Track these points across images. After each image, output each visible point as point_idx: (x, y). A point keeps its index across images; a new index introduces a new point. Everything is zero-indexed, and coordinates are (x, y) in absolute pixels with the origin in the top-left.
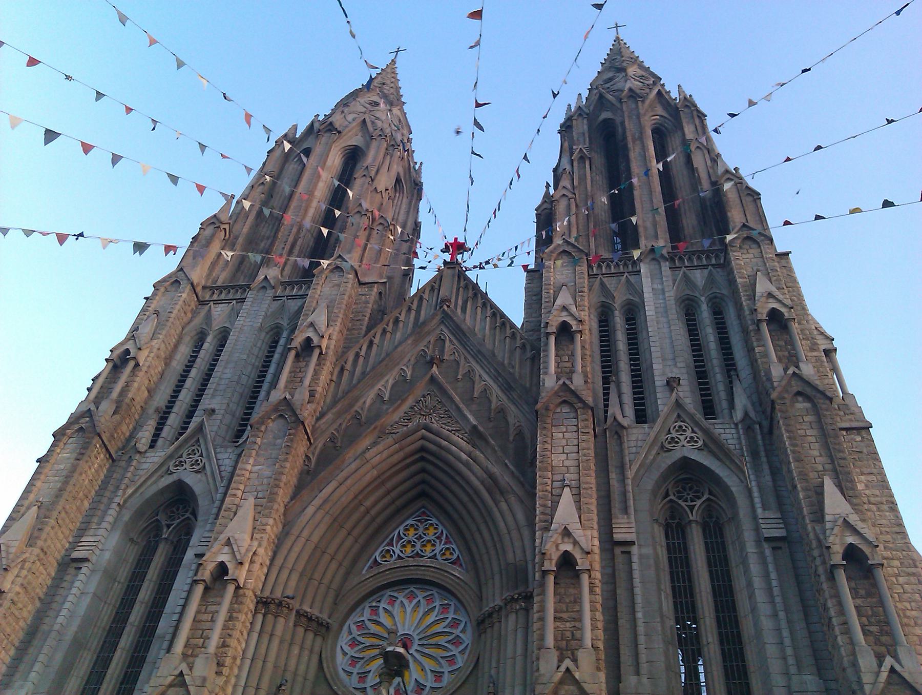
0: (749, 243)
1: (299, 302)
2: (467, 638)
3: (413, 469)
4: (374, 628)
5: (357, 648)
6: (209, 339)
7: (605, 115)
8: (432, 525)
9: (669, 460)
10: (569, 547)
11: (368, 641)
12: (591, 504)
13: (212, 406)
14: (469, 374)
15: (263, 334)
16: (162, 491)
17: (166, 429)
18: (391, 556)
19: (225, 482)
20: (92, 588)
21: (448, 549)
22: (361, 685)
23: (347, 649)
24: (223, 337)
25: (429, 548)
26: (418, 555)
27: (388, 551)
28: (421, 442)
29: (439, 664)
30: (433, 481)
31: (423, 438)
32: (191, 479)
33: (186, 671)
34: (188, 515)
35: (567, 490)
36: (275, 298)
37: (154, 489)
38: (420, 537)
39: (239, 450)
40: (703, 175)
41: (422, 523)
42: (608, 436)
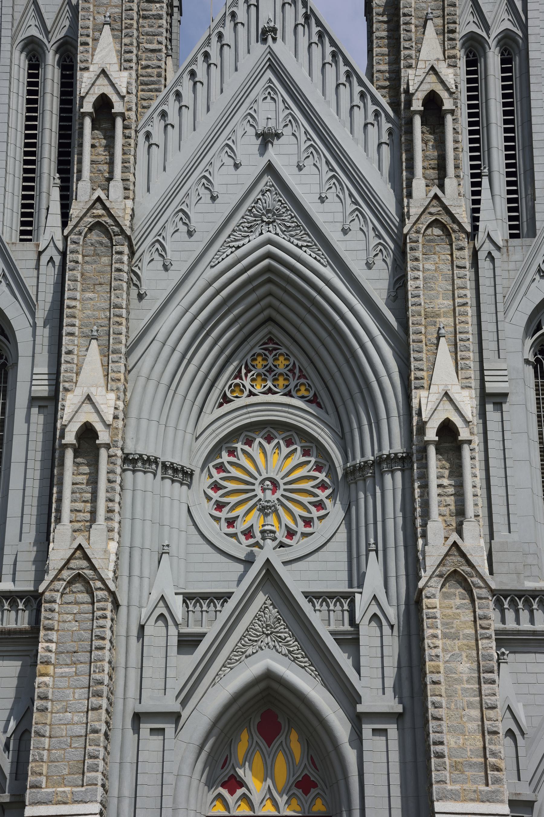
3: (261, 292)
4: (235, 472)
5: (221, 492)
8: (281, 354)
11: (231, 486)
12: (468, 359)
15: (16, 53)
18: (242, 391)
21: (302, 384)
22: (231, 530)
23: (210, 492)
25: (281, 382)
26: (270, 391)
27: (237, 385)
29: (309, 512)
30: (282, 307)
31: (269, 255)
33: (85, 545)
35: (442, 339)
38: (270, 370)
41: (270, 352)
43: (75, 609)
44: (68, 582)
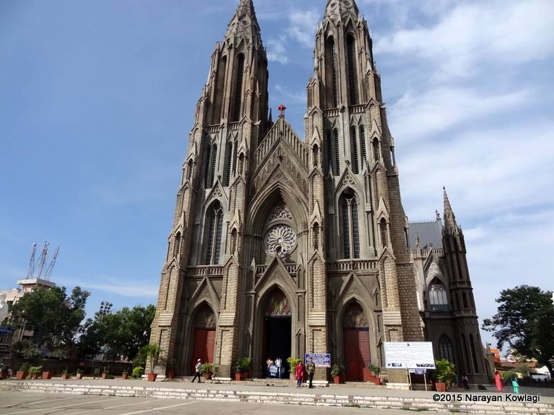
2: (295, 238)
7: (330, 33)
9: (344, 187)
10: (316, 221)
13: (218, 175)
14: (289, 161)
32: (219, 199)
36: (228, 131)
40: (363, 67)
42: (328, 183)
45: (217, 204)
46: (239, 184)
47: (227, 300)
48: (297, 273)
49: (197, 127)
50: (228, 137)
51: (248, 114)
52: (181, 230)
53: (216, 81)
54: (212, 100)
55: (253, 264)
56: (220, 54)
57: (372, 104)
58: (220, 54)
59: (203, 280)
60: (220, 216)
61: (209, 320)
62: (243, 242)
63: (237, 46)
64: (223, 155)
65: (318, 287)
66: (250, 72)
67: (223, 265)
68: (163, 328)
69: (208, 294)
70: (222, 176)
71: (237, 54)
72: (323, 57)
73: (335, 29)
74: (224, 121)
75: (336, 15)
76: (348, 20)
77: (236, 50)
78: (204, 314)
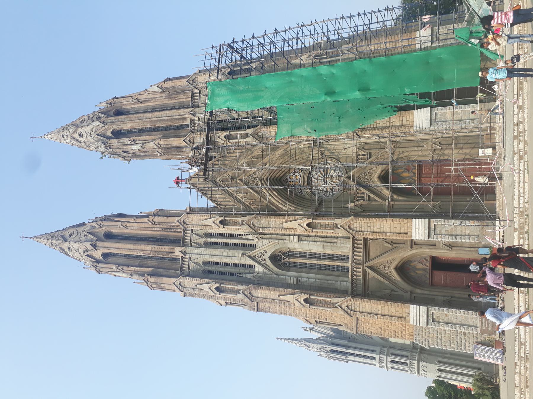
0: (195, 80)
1: (194, 236)
6: (207, 268)
7: (109, 133)
13: (240, 255)
16: (272, 263)
17: (246, 271)
19: (272, 240)
20: (305, 275)
24: (206, 263)
28: (265, 179)
32: (269, 254)
34: (281, 254)
36: (191, 246)
37: (272, 266)
39: (261, 239)
43: (358, 227)
44: (350, 229)
45: (274, 258)
46: (256, 225)
47: (395, 231)
48: (367, 151)
49: (178, 285)
50: (199, 245)
51: (177, 219)
52: (302, 297)
53: (128, 266)
54: (150, 269)
55: (352, 205)
56: (98, 261)
57: (193, 81)
58: (98, 261)
59: (368, 270)
60: (290, 254)
61: (420, 266)
62: (325, 216)
63: (95, 239)
64: (217, 251)
65: (385, 122)
66: (129, 222)
67: (350, 246)
68: (431, 319)
69: (387, 265)
70: (242, 251)
71: (104, 239)
72: (132, 139)
73: (106, 127)
74: (178, 251)
75: (92, 130)
76: (100, 115)
77: (99, 239)
78: (413, 274)
